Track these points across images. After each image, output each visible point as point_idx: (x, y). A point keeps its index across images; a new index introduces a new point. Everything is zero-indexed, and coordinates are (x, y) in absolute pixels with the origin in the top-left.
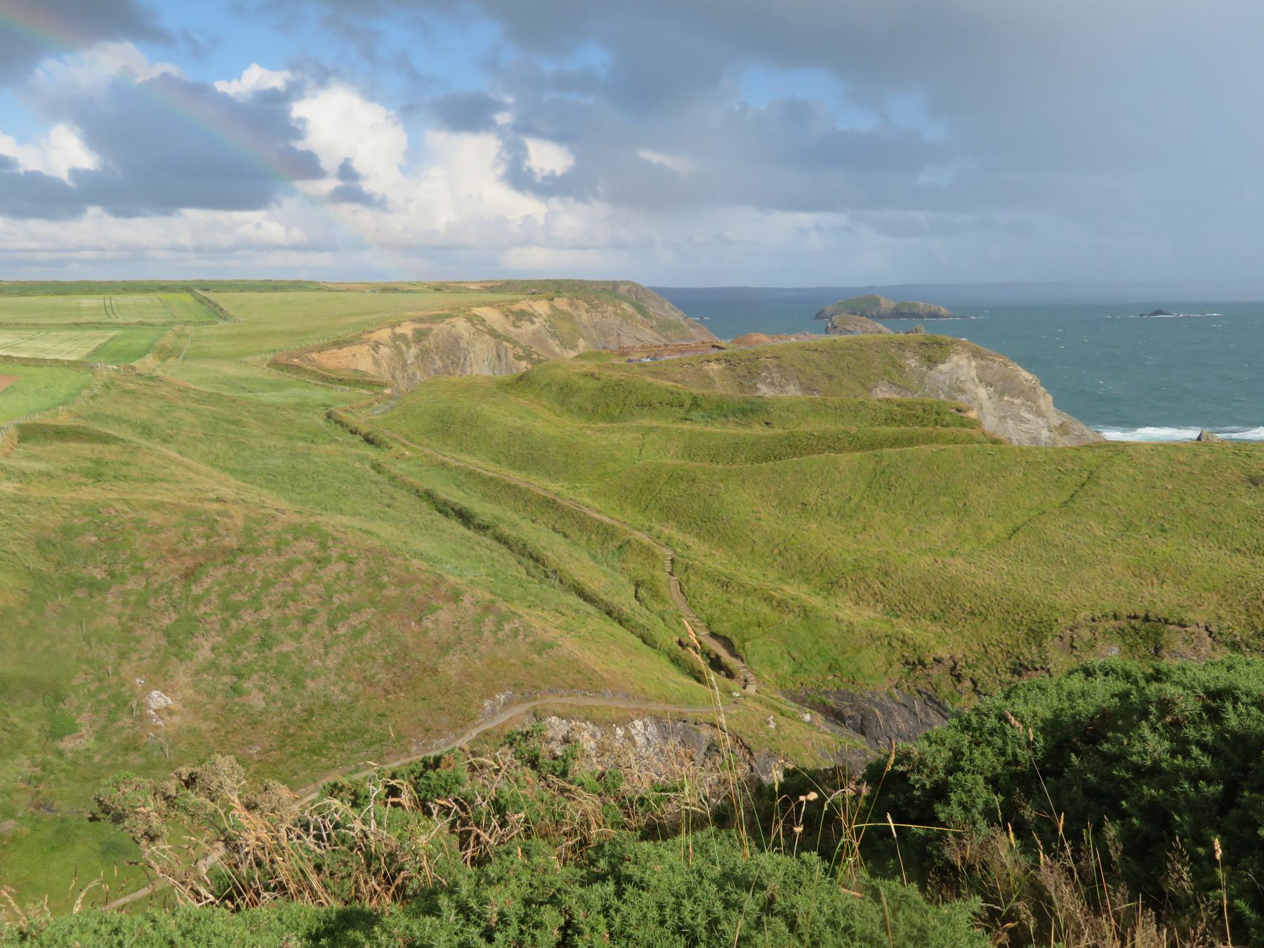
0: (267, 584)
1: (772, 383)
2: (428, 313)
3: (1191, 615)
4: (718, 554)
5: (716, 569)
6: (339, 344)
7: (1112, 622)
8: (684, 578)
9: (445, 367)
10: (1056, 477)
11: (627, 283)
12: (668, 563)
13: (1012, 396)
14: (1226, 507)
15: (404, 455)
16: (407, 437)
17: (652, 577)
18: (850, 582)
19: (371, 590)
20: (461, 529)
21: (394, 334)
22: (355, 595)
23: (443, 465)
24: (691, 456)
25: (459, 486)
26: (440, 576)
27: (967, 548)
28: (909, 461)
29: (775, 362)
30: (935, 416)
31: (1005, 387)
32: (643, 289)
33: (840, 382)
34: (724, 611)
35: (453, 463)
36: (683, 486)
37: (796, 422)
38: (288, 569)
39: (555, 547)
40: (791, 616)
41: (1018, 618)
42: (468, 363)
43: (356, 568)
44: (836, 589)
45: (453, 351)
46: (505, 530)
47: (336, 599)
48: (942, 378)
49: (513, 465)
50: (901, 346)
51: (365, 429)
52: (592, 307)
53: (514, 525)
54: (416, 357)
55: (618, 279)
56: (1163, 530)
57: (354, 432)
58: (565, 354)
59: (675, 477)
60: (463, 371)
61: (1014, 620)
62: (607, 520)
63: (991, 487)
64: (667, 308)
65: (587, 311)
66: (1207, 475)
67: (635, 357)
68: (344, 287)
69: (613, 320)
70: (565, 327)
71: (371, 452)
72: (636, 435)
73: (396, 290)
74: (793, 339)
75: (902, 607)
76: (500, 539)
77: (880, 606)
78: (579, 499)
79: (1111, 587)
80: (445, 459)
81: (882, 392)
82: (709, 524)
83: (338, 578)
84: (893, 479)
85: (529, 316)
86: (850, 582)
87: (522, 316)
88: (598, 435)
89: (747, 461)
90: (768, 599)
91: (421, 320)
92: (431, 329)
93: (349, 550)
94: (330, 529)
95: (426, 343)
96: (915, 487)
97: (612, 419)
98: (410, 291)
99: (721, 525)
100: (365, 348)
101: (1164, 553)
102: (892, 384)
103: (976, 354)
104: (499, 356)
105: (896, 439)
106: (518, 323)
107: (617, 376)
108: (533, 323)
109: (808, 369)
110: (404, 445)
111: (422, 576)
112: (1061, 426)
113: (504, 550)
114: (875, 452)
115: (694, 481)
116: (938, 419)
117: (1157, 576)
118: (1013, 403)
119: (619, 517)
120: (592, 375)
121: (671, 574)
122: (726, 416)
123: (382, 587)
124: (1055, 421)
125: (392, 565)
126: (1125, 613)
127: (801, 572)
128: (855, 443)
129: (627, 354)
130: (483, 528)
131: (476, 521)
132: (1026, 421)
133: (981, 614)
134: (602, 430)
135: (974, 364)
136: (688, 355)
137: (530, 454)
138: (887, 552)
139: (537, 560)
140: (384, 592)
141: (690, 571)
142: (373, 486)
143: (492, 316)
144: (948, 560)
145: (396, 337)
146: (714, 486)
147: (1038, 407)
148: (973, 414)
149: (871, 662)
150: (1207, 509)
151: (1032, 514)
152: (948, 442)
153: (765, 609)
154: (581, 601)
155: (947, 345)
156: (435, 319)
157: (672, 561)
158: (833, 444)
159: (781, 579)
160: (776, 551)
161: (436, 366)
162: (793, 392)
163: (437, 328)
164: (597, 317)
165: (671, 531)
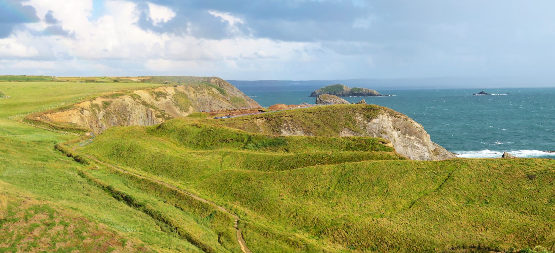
0: (19, 238)
1: (289, 129)
2: (110, 93)
3: (501, 246)
4: (261, 218)
5: (261, 226)
6: (61, 109)
7: (462, 250)
8: (244, 231)
9: (119, 121)
10: (432, 176)
11: (216, 78)
12: (236, 223)
13: (410, 135)
14: (517, 191)
15: (96, 167)
16: (98, 158)
17: (228, 230)
18: (330, 231)
19: (77, 240)
20: (126, 207)
21: (92, 104)
22: (68, 243)
23: (117, 172)
24: (248, 167)
25: (126, 184)
26: (114, 232)
27: (389, 213)
28: (358, 169)
29: (290, 118)
30: (371, 146)
31: (407, 131)
32: (223, 81)
33: (323, 129)
34: (265, 248)
35: (122, 172)
36: (243, 182)
37: (301, 149)
38: (31, 229)
39: (177, 215)
40: (300, 249)
41: (415, 248)
42: (131, 119)
43: (69, 228)
44: (322, 235)
45: (123, 114)
46: (150, 207)
47: (58, 246)
48: (374, 126)
49: (154, 173)
50: (354, 110)
51: (75, 154)
52: (196, 90)
53: (154, 204)
54: (104, 116)
55: (210, 76)
56: (486, 203)
57: (69, 156)
58: (182, 114)
59: (239, 178)
60: (129, 123)
61: (413, 250)
62: (204, 201)
63: (400, 182)
64: (235, 91)
65: (194, 92)
66: (507, 175)
67: (219, 116)
68: (65, 79)
69: (208, 97)
70: (182, 100)
71: (79, 166)
72: (219, 156)
73: (93, 81)
74: (299, 107)
75: (357, 244)
76: (147, 212)
77: (345, 244)
78: (189, 190)
79: (461, 232)
80: (118, 170)
81: (345, 134)
82: (257, 203)
83: (59, 234)
84: (351, 178)
85: (164, 95)
86: (330, 231)
87: (160, 94)
88: (200, 156)
89: (276, 169)
90: (288, 241)
91: (107, 97)
92: (112, 102)
93: (65, 219)
94: (55, 208)
95: (109, 109)
96: (362, 182)
97: (206, 147)
98: (101, 82)
99: (263, 203)
100: (76, 112)
101: (487, 214)
102: (349, 129)
103: (391, 114)
104: (148, 116)
105: (352, 158)
106: (158, 99)
107: (209, 126)
108: (166, 98)
109: (307, 122)
110: (96, 162)
111: (105, 232)
112: (435, 150)
113: (149, 217)
114: (341, 164)
115: (249, 180)
116: (373, 147)
117: (484, 226)
118: (410, 139)
119: (210, 199)
120: (197, 125)
121: (237, 229)
122: (266, 146)
123: (83, 238)
124: (432, 148)
125: (89, 226)
126: (468, 245)
127: (305, 227)
128: (332, 160)
129: (214, 115)
130: (138, 206)
131: (134, 202)
132: (415, 148)
133: (396, 247)
134: (201, 154)
135: (390, 119)
136: (246, 115)
137: (164, 167)
138: (348, 216)
139: (167, 223)
140: (84, 241)
141: (247, 227)
142: (79, 184)
143: (145, 95)
144: (380, 219)
145: (93, 106)
146: (259, 182)
147: (423, 141)
148: (390, 145)
150: (508, 191)
151: (421, 195)
152: (378, 159)
153: (286, 246)
154: (190, 244)
155: (377, 109)
156: (114, 96)
157: (238, 222)
158: (320, 160)
159: (294, 230)
160: (292, 216)
161: (114, 121)
162: (299, 134)
163: (115, 101)
164: (199, 95)
165: (237, 206)
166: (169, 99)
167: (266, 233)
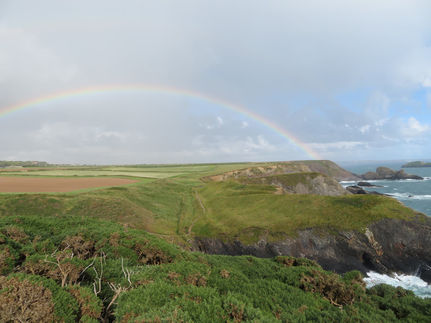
85: (270, 169)
132: (333, 191)
143: (261, 169)
149: (214, 233)
165: (209, 210)
166: (272, 170)
167: (205, 219)
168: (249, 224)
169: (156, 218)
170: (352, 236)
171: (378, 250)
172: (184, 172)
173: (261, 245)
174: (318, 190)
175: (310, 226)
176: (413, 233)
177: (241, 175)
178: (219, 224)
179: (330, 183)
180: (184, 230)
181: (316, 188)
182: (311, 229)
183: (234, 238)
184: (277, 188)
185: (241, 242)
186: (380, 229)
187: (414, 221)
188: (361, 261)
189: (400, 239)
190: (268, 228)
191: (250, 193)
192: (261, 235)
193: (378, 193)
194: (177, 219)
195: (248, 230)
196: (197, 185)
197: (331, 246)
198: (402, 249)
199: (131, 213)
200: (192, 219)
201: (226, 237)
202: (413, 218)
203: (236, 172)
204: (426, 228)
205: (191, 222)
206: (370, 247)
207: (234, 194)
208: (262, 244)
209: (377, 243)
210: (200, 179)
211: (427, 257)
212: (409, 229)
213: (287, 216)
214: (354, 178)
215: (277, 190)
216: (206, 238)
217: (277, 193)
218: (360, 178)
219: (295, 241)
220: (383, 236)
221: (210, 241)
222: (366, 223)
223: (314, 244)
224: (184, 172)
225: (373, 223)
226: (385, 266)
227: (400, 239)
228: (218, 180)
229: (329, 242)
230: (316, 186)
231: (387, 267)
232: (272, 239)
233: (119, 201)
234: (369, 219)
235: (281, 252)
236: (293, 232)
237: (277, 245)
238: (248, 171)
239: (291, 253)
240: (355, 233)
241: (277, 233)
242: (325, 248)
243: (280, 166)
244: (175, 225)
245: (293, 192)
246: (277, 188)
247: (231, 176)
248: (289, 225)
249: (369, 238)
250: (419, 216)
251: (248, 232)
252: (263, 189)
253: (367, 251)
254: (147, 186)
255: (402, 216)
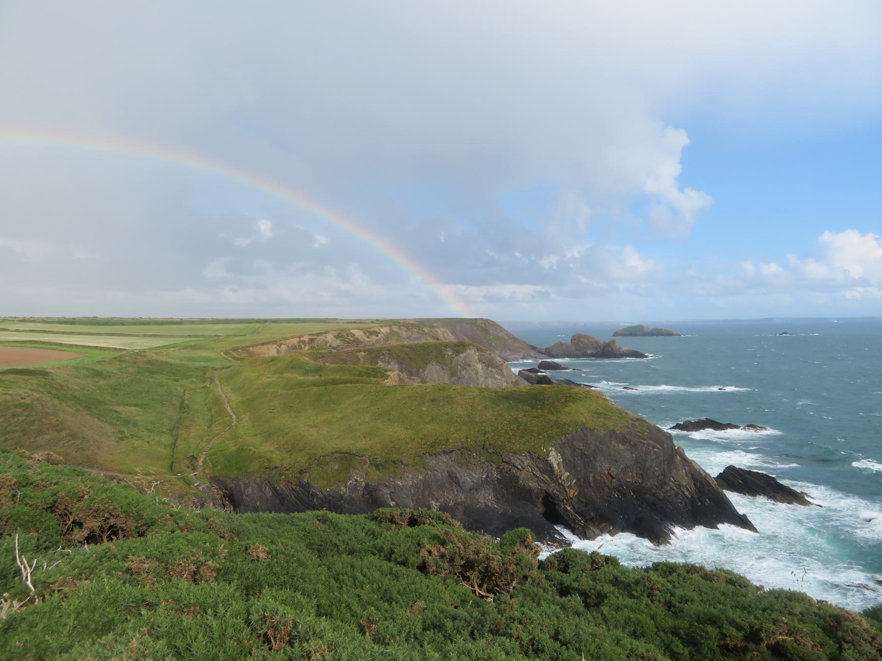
85: (376, 333)
108: (377, 336)
132: (496, 379)
143: (358, 334)
165: (246, 418)
166: (380, 336)
167: (235, 437)
168: (331, 446)
169: (121, 439)
170: (526, 464)
171: (570, 487)
172: (190, 336)
173: (354, 488)
174: (467, 377)
175: (450, 447)
176: (627, 454)
177: (315, 344)
178: (267, 448)
179: (490, 364)
180: (187, 462)
181: (463, 373)
182: (451, 452)
183: (298, 475)
184: (389, 373)
185: (312, 483)
186: (574, 449)
187: (630, 433)
188: (541, 509)
189: (606, 466)
190: (368, 454)
191: (334, 382)
192: (354, 468)
193: (573, 383)
194: (171, 440)
195: (327, 459)
196: (218, 365)
197: (488, 483)
198: (609, 484)
199: (58, 428)
200: (205, 439)
201: (281, 475)
202: (628, 427)
203: (306, 339)
204: (648, 445)
205: (203, 444)
206: (556, 482)
207: (300, 384)
208: (355, 485)
209: (568, 474)
210: (226, 353)
211: (647, 496)
212: (621, 447)
213: (407, 429)
214: (532, 354)
215: (388, 376)
216: (236, 479)
217: (388, 382)
218: (542, 353)
219: (421, 477)
220: (578, 461)
221: (245, 484)
222: (550, 438)
223: (457, 482)
224: (190, 336)
225: (563, 438)
226: (580, 515)
227: (606, 466)
228: (267, 355)
229: (484, 476)
230: (464, 369)
231: (583, 517)
232: (375, 476)
233: (28, 400)
234: (556, 430)
235: (393, 500)
236: (418, 460)
237: (386, 486)
238: (330, 337)
239: (413, 501)
240: (532, 458)
241: (386, 461)
242: (476, 488)
243: (395, 328)
244: (167, 452)
245: (419, 380)
246: (389, 373)
247: (294, 348)
248: (410, 446)
249: (555, 465)
250: (637, 423)
251: (328, 463)
252: (360, 375)
253: (550, 491)
254: (99, 367)
255: (610, 424)
